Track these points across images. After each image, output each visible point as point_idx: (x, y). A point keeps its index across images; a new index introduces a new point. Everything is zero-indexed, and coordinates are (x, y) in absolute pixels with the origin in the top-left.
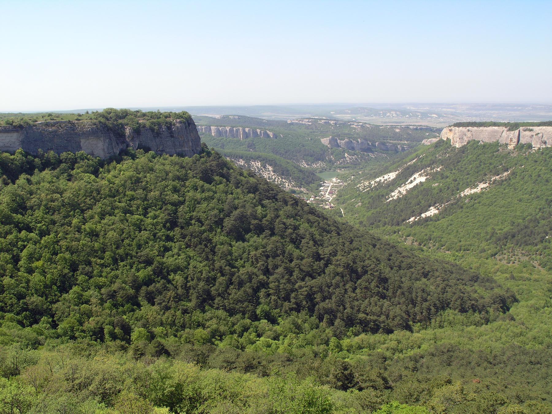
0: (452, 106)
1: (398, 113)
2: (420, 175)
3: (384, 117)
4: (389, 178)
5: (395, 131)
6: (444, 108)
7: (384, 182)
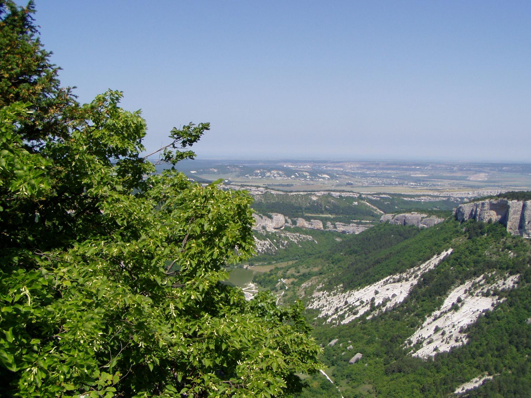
0: (338, 165)
1: (280, 172)
2: (470, 293)
3: (263, 177)
4: (394, 296)
5: (311, 200)
6: (329, 166)
7: (384, 304)
